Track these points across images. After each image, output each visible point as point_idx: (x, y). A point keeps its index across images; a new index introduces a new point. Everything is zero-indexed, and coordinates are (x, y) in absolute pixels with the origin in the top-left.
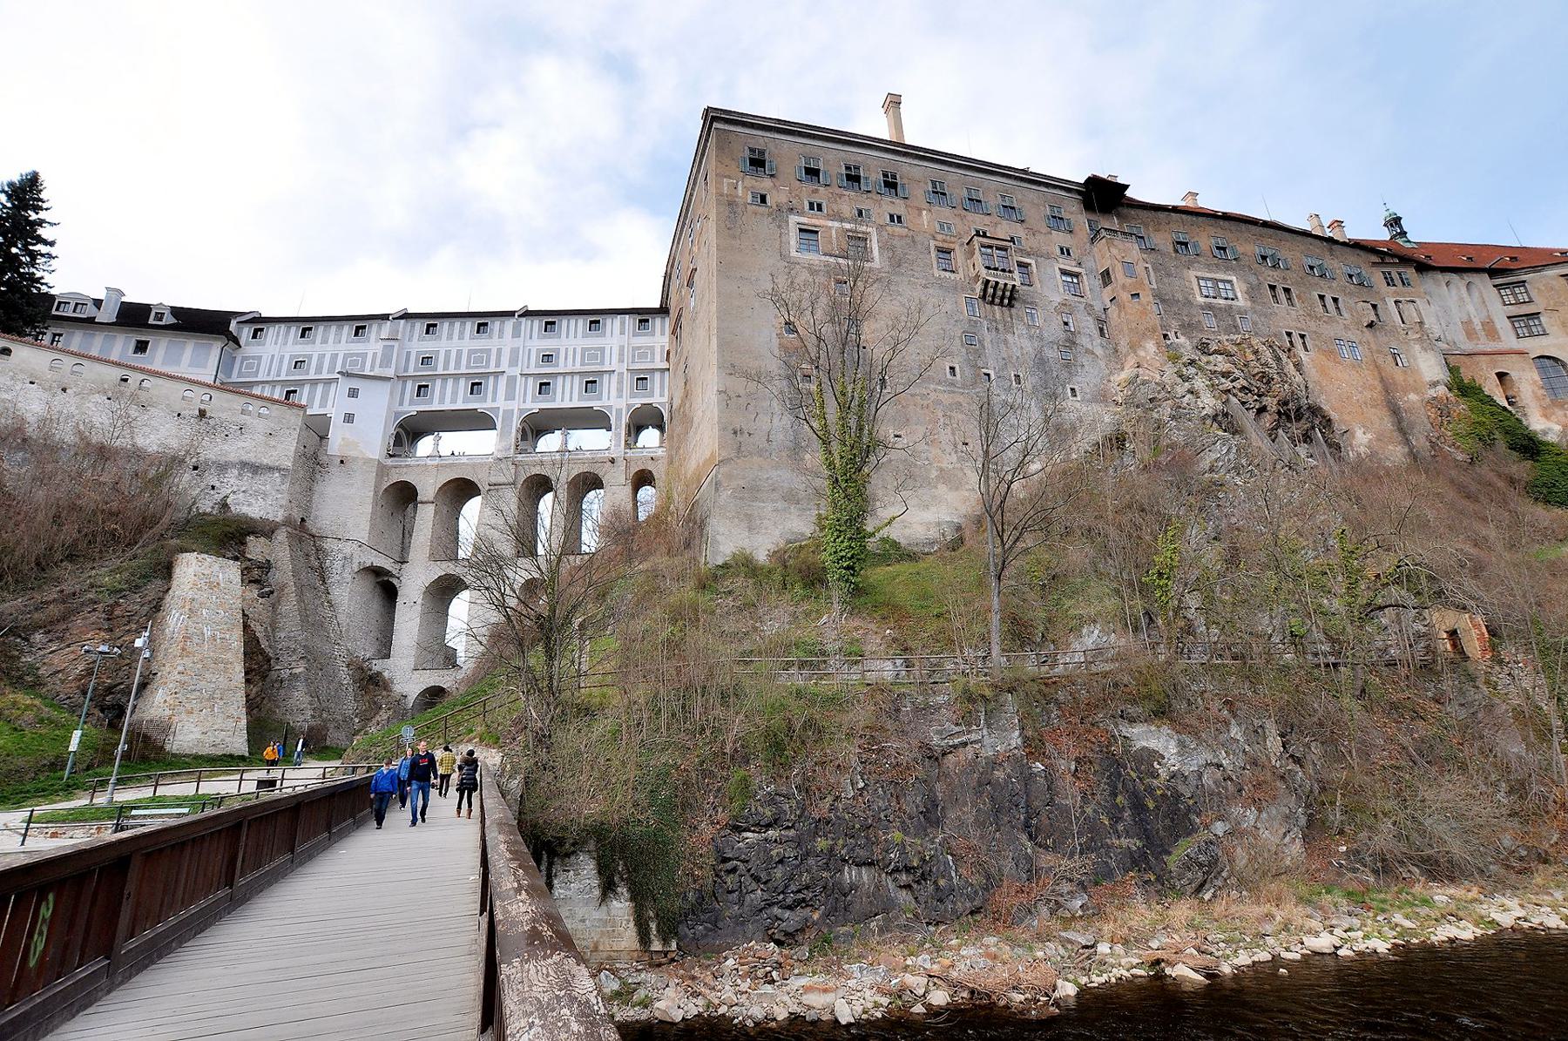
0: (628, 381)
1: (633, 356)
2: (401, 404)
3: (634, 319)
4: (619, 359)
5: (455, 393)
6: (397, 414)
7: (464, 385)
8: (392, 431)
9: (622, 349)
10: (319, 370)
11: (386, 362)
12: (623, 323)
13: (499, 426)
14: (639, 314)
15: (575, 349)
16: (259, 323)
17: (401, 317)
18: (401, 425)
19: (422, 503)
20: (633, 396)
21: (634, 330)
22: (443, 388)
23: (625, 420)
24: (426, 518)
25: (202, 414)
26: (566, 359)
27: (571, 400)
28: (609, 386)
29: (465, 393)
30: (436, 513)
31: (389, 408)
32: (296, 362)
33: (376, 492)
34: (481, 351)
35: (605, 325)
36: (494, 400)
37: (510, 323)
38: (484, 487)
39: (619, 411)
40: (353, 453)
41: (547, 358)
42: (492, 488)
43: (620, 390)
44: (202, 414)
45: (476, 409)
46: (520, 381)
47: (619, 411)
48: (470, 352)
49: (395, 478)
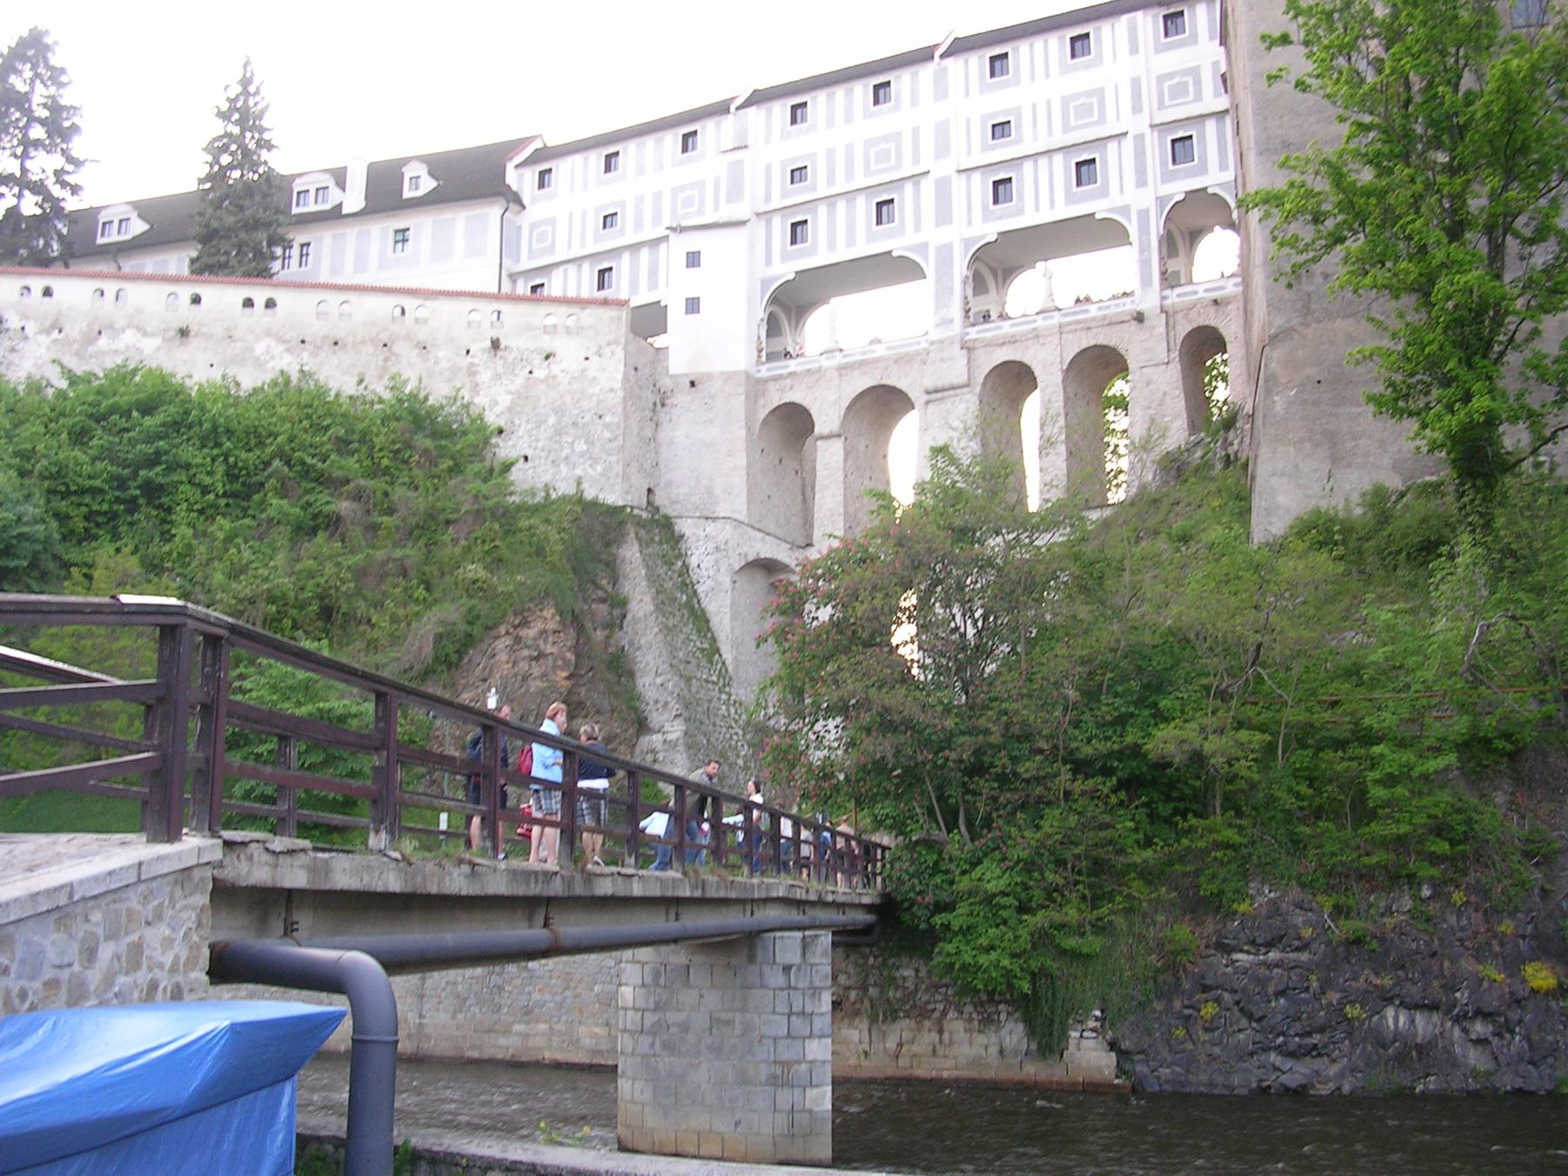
0: (1157, 149)
1: (1161, 95)
2: (768, 262)
3: (1155, 17)
5: (851, 228)
6: (765, 283)
7: (864, 208)
8: (761, 313)
9: (1136, 84)
10: (639, 224)
12: (1132, 30)
16: (544, 158)
17: (748, 103)
18: (775, 300)
19: (822, 438)
20: (1167, 177)
21: (1156, 40)
23: (1156, 228)
24: (829, 458)
25: (495, 344)
27: (1052, 205)
28: (1116, 163)
30: (847, 454)
32: (605, 217)
33: (749, 429)
35: (1099, 39)
37: (927, 71)
38: (916, 395)
39: (1143, 215)
41: (1000, 129)
42: (933, 396)
44: (495, 344)
46: (959, 183)
47: (1143, 215)
48: (869, 144)
49: (775, 399)
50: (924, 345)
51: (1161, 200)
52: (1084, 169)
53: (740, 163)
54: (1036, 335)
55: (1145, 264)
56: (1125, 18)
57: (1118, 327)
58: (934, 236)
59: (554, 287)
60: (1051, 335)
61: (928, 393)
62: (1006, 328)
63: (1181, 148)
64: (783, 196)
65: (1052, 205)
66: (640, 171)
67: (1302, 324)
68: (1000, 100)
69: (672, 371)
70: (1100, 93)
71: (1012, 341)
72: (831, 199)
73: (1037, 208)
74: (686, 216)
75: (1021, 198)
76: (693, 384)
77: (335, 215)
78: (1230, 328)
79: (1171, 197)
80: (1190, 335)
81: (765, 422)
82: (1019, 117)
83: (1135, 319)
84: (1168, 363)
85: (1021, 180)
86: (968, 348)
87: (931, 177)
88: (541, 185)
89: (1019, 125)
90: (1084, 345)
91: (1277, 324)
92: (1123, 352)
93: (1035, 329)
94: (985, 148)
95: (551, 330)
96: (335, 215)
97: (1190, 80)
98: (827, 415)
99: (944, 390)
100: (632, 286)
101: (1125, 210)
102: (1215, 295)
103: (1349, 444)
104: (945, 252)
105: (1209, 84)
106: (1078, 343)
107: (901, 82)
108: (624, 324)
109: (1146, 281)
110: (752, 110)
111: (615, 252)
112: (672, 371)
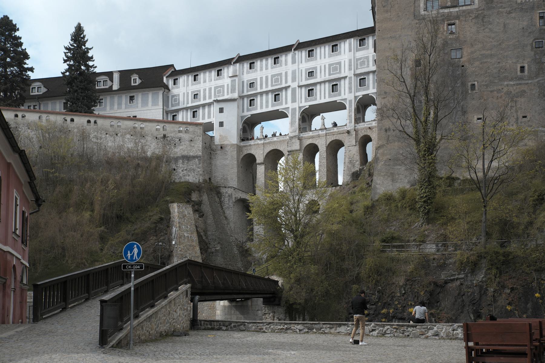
0: (355, 81)
2: (243, 112)
4: (349, 68)
5: (267, 102)
6: (242, 117)
7: (271, 97)
8: (241, 127)
11: (233, 91)
12: (350, 44)
13: (290, 115)
14: (359, 36)
15: (325, 66)
18: (245, 122)
22: (261, 100)
26: (321, 72)
27: (325, 98)
28: (344, 86)
29: (272, 101)
31: (238, 115)
33: (238, 161)
34: (277, 75)
36: (286, 103)
37: (290, 56)
39: (350, 101)
40: (226, 143)
42: (290, 153)
43: (350, 88)
45: (278, 110)
47: (350, 101)
48: (273, 76)
49: (245, 152)
50: (288, 138)
51: (356, 97)
52: (334, 87)
53: (235, 80)
54: (319, 136)
55: (350, 116)
56: (348, 40)
57: (342, 135)
58: (290, 105)
59: (180, 117)
60: (323, 136)
61: (288, 152)
62: (311, 134)
63: (362, 82)
64: (247, 92)
65: (325, 98)
66: (205, 82)
67: (386, 144)
68: (311, 65)
69: (216, 143)
70: (339, 63)
71: (312, 137)
72: (261, 94)
73: (320, 99)
74: (219, 96)
75: (316, 95)
76: (221, 148)
77: (109, 91)
78: (374, 136)
79: (359, 96)
80: (362, 137)
81: (242, 159)
82: (316, 70)
83: (347, 133)
84: (355, 146)
85: (316, 89)
86: (300, 139)
87: (290, 89)
88: (175, 84)
89: (316, 72)
90: (333, 139)
91: (380, 143)
92: (343, 142)
93: (319, 134)
94: (306, 79)
95: (180, 132)
96: (109, 91)
97: (366, 60)
98: (260, 158)
99: (293, 151)
100: (203, 118)
101: (345, 99)
102: (369, 126)
103: (397, 176)
104: (294, 110)
105: (371, 62)
106: (330, 139)
107: (283, 58)
108: (202, 130)
109: (350, 122)
110: (238, 65)
111: (198, 107)
112: (216, 143)
